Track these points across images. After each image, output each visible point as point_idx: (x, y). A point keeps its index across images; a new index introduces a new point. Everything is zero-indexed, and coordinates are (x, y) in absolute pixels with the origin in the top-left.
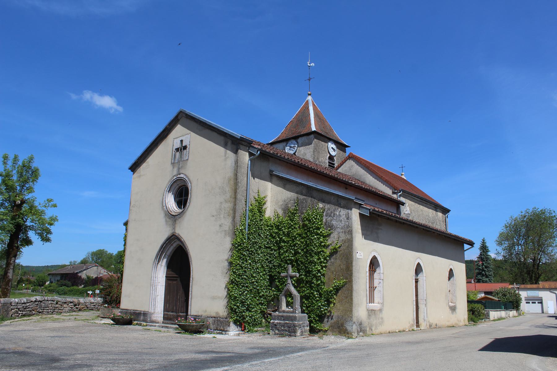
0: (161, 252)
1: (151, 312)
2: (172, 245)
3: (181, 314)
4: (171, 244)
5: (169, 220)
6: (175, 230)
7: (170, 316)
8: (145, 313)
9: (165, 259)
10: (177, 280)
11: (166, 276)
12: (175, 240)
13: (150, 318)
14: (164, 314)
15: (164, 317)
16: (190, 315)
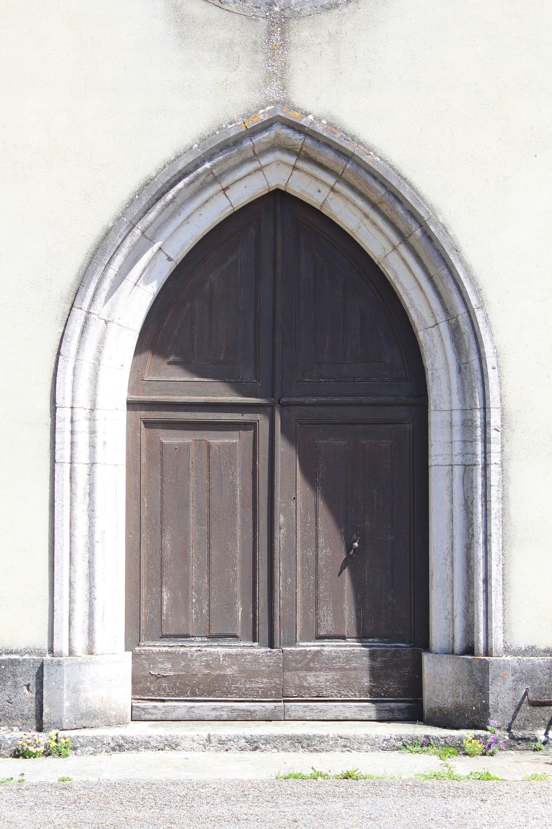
0: (137, 232)
1: (71, 653)
2: (224, 190)
3: (312, 646)
4: (224, 184)
5: (215, 12)
6: (284, 88)
7: (208, 666)
8: (13, 662)
9: (147, 282)
10: (252, 426)
11: (132, 405)
12: (264, 161)
13: (76, 691)
14: (135, 656)
15: (135, 681)
16: (507, 650)
